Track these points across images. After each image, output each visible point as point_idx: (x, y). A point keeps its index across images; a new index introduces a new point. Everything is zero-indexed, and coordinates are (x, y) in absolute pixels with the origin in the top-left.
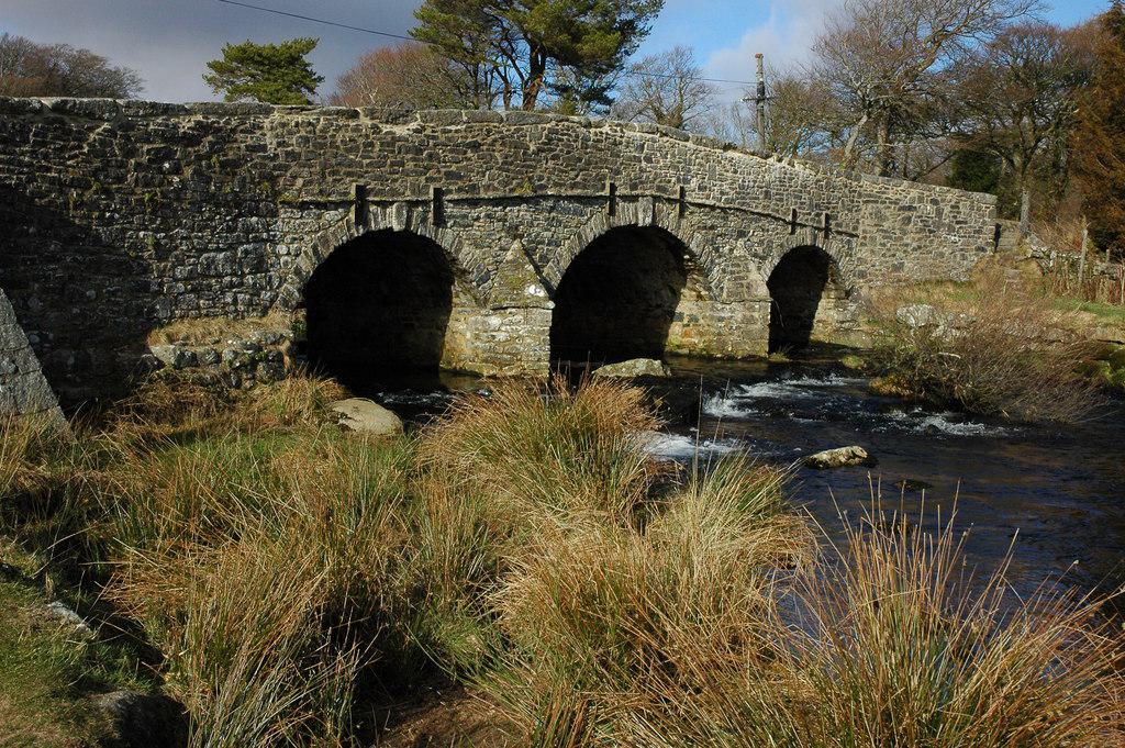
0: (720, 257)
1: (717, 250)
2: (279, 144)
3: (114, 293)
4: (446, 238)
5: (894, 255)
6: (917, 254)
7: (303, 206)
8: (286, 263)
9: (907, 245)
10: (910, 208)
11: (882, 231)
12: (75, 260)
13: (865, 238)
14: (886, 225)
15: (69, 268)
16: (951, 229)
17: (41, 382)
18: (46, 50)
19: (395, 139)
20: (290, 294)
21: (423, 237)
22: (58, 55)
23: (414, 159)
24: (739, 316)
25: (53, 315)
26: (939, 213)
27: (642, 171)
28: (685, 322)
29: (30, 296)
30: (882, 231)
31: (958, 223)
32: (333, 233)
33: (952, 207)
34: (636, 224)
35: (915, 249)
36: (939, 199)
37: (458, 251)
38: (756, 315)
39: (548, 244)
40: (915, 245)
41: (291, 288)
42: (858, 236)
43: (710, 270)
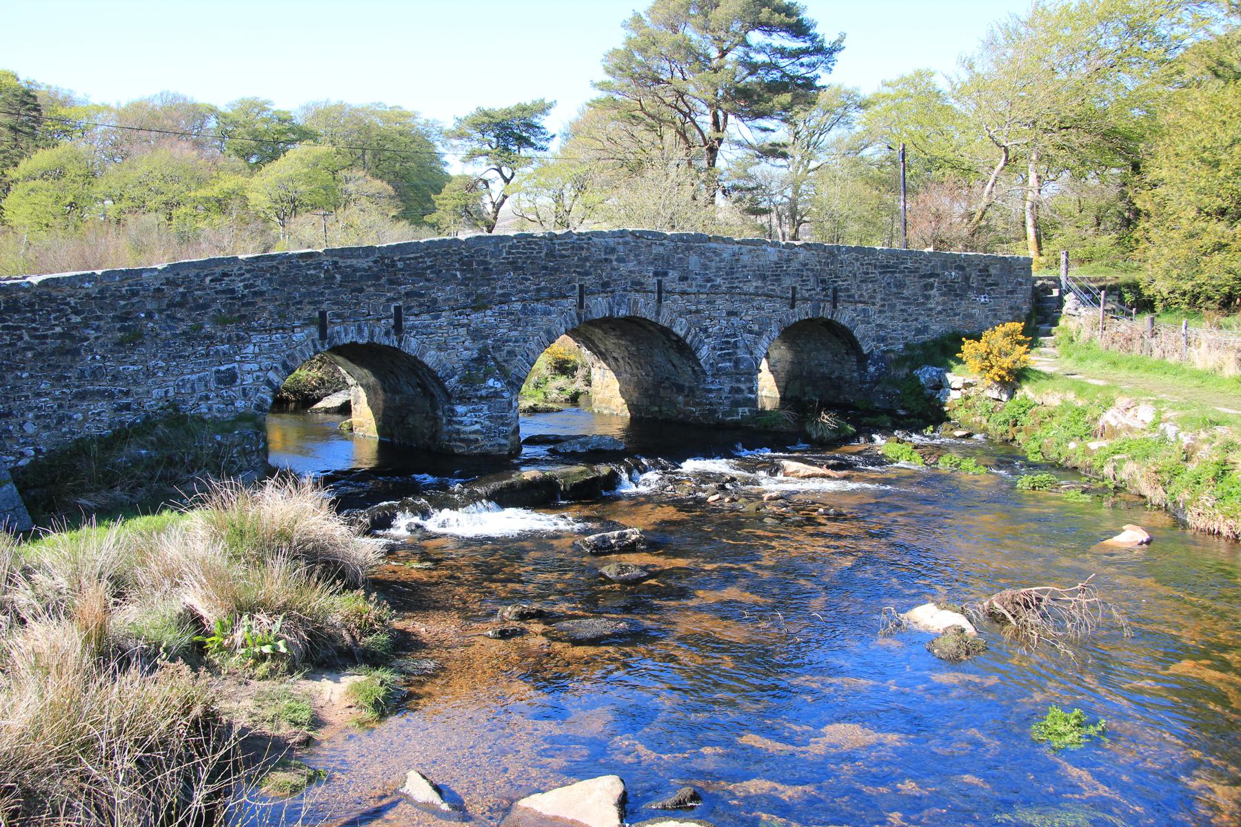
0: (708, 337)
1: (705, 330)
2: (246, 287)
3: (99, 414)
4: (412, 345)
5: (916, 320)
6: (942, 317)
7: (270, 331)
8: (258, 377)
9: (931, 309)
10: (931, 275)
11: (903, 298)
12: (63, 393)
13: (883, 306)
14: (906, 292)
15: (57, 399)
16: (980, 291)
17: (12, 489)
18: (362, 110)
19: (355, 270)
20: (264, 401)
21: (388, 347)
22: (373, 113)
23: (373, 285)
24: (727, 388)
25: (45, 434)
26: (967, 279)
27: (613, 269)
28: (686, 392)
29: (25, 422)
30: (903, 298)
31: (987, 285)
32: (301, 351)
33: (980, 271)
34: (611, 316)
35: (940, 313)
36: (965, 265)
37: (423, 354)
38: (743, 386)
39: (516, 341)
40: (940, 308)
41: (264, 396)
42: (874, 304)
43: (698, 349)
